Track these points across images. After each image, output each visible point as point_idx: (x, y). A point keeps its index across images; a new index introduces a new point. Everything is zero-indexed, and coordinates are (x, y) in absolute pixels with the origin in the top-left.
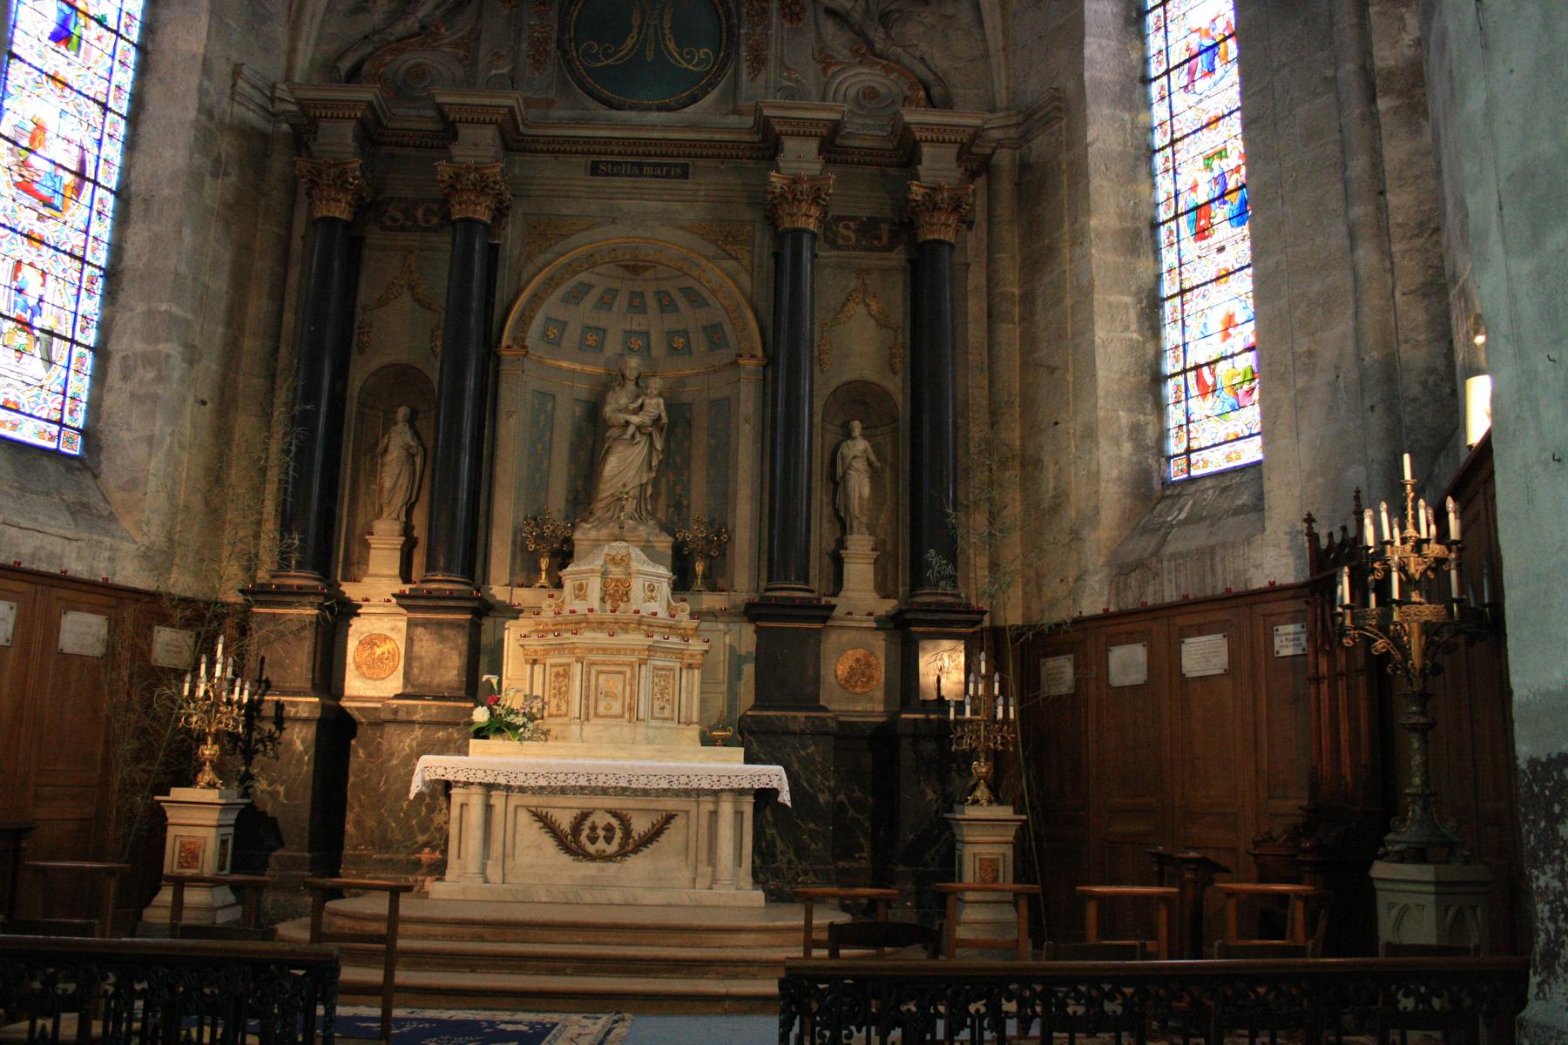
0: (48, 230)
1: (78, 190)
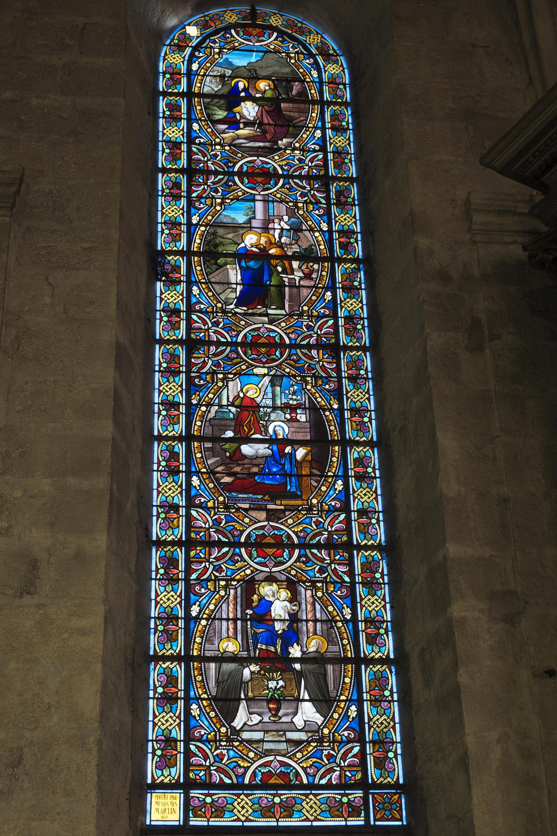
0: (289, 528)
1: (319, 461)
